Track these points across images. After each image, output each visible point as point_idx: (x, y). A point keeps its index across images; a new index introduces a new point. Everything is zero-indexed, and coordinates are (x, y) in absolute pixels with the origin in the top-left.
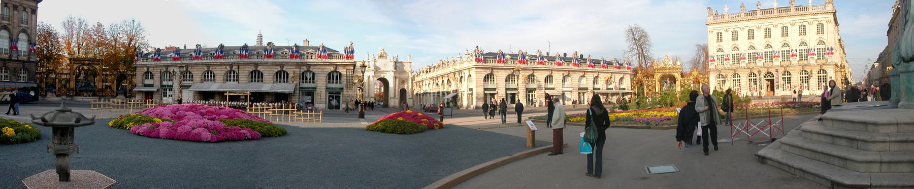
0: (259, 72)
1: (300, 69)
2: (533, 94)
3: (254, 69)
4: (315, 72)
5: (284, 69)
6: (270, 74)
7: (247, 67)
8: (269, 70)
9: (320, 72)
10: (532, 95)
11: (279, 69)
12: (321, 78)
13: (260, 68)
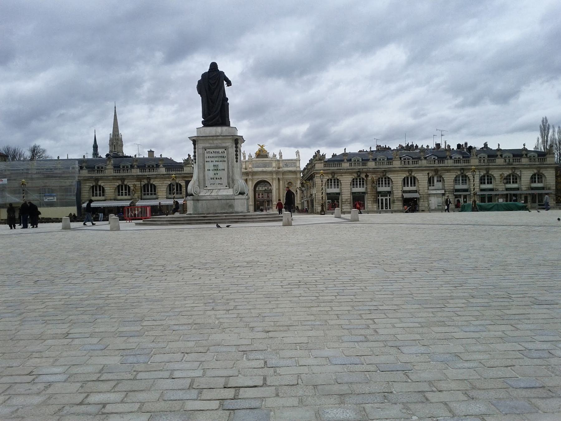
0: (100, 186)
1: (141, 182)
2: (388, 198)
3: (94, 184)
4: (156, 185)
5: (125, 183)
6: (111, 188)
7: (87, 182)
8: (110, 184)
9: (161, 185)
10: (386, 199)
11: (120, 183)
12: (162, 189)
13: (101, 183)
